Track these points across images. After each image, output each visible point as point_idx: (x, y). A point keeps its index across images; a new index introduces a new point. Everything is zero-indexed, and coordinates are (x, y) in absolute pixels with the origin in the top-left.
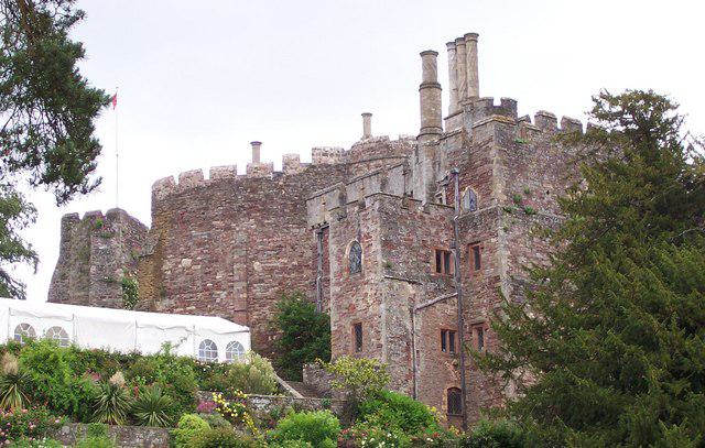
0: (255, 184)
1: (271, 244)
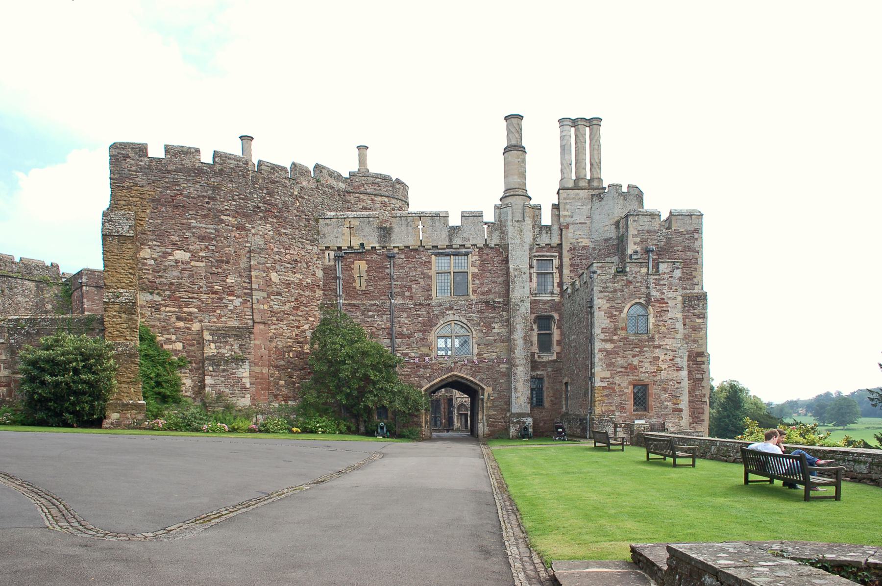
0: (271, 186)
1: (288, 256)
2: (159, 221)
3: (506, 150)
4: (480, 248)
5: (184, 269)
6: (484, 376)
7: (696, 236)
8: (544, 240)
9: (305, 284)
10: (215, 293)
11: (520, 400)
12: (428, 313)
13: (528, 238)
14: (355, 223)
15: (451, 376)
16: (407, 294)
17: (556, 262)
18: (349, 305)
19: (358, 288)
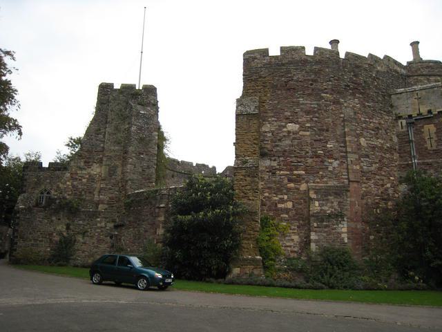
2: (276, 102)
5: (294, 138)
10: (318, 156)
18: (423, 163)
19: (429, 148)
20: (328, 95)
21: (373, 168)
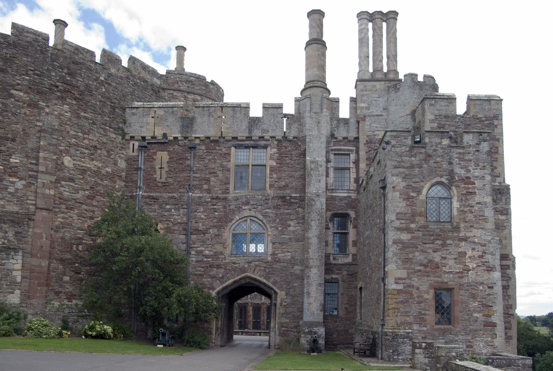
0: (73, 66)
1: (86, 141)
3: (308, 44)
4: (279, 141)
6: (278, 279)
7: (496, 122)
8: (341, 133)
9: (103, 172)
11: (313, 306)
12: (225, 207)
13: (325, 130)
14: (161, 112)
15: (244, 278)
16: (205, 187)
17: (353, 156)
18: (148, 197)
19: (158, 180)
20: (22, 94)
21: (79, 196)
